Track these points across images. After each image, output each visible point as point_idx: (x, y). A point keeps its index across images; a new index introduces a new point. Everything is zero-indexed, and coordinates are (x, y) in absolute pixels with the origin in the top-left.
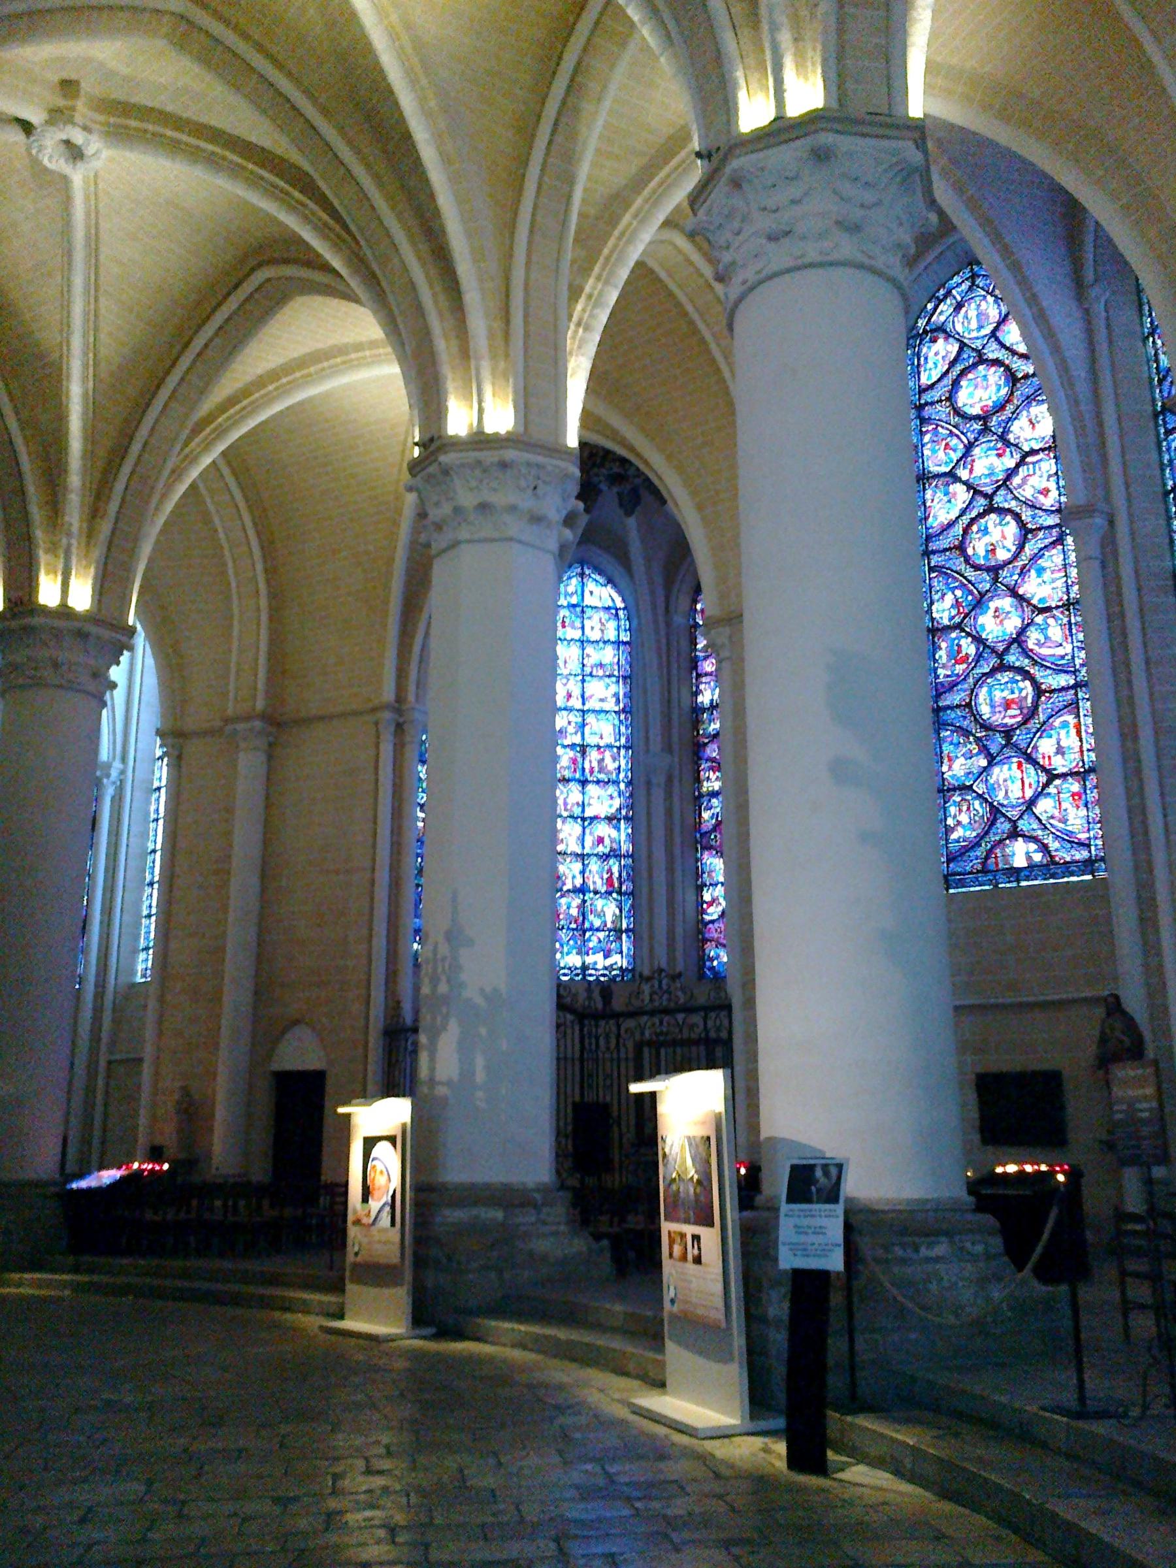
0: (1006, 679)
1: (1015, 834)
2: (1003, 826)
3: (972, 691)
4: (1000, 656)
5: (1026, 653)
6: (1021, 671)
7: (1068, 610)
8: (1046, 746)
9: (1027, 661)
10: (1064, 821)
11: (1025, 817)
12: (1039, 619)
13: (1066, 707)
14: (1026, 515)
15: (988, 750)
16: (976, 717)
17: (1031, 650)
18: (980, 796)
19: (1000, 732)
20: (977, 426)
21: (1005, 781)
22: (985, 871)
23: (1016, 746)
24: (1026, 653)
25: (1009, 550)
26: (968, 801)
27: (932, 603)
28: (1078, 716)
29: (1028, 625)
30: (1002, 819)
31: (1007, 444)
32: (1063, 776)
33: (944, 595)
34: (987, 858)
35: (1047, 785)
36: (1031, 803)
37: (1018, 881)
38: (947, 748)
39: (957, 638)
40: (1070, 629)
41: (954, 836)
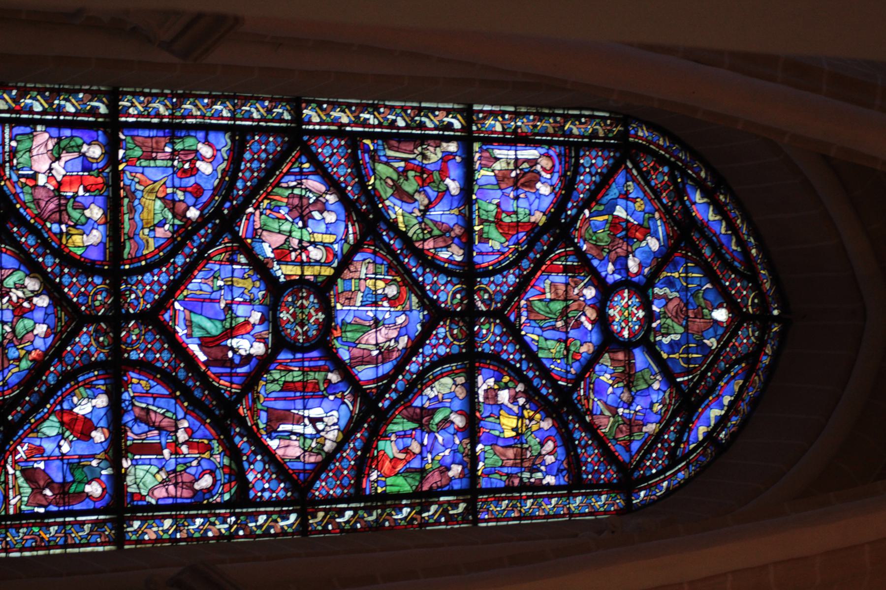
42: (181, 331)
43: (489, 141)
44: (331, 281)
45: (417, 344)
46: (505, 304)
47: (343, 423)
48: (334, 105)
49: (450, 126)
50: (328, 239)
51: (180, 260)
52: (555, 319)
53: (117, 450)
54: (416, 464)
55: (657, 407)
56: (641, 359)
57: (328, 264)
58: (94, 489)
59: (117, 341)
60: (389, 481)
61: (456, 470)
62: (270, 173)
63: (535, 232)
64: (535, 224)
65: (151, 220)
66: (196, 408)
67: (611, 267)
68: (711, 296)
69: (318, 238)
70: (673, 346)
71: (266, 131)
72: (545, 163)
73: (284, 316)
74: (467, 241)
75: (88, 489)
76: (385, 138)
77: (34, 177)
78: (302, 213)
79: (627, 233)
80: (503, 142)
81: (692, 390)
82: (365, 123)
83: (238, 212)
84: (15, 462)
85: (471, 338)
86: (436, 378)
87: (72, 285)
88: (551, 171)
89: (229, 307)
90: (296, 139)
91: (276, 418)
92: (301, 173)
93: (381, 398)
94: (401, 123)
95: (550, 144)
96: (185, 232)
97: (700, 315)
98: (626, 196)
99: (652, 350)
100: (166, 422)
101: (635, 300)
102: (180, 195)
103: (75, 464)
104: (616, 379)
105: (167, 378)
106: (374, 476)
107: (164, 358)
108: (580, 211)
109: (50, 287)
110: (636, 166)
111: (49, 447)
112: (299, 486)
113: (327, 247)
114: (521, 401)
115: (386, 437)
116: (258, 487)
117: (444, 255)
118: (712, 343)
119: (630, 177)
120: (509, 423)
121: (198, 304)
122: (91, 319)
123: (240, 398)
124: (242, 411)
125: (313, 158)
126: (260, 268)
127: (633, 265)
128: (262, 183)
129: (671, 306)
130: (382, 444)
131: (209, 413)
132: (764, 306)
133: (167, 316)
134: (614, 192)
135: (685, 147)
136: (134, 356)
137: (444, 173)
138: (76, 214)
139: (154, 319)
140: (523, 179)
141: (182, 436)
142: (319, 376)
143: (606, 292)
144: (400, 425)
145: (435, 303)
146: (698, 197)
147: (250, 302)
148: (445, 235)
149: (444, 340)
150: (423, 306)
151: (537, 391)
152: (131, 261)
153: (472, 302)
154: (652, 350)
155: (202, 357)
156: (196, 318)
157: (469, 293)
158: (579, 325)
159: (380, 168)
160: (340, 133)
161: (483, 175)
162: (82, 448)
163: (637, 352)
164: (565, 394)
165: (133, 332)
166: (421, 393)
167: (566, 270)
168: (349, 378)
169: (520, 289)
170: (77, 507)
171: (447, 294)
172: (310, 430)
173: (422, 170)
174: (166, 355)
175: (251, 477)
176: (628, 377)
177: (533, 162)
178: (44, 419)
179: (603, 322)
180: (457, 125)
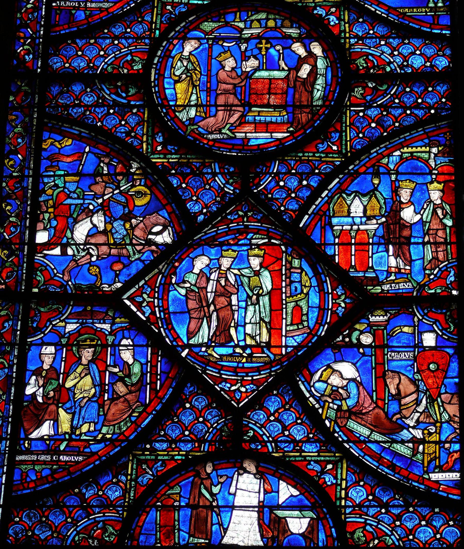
2: (199, 419)
3: (155, 44)
10: (391, 427)
11: (273, 404)
13: (420, 123)
15: (181, 204)
16: (160, 115)
18: (138, 327)
19: (223, 160)
21: (224, 292)
23: (263, 206)
30: (201, 402)
32: (400, 304)
34: (138, 507)
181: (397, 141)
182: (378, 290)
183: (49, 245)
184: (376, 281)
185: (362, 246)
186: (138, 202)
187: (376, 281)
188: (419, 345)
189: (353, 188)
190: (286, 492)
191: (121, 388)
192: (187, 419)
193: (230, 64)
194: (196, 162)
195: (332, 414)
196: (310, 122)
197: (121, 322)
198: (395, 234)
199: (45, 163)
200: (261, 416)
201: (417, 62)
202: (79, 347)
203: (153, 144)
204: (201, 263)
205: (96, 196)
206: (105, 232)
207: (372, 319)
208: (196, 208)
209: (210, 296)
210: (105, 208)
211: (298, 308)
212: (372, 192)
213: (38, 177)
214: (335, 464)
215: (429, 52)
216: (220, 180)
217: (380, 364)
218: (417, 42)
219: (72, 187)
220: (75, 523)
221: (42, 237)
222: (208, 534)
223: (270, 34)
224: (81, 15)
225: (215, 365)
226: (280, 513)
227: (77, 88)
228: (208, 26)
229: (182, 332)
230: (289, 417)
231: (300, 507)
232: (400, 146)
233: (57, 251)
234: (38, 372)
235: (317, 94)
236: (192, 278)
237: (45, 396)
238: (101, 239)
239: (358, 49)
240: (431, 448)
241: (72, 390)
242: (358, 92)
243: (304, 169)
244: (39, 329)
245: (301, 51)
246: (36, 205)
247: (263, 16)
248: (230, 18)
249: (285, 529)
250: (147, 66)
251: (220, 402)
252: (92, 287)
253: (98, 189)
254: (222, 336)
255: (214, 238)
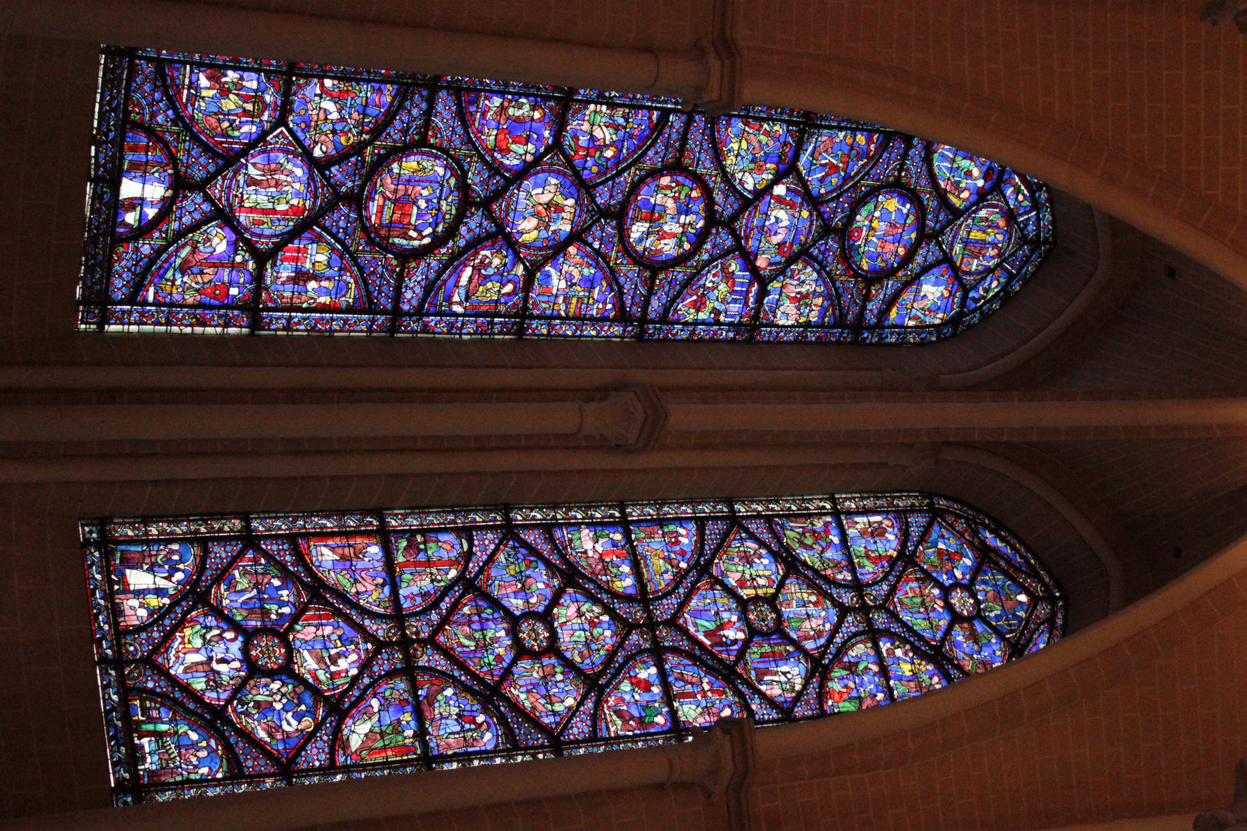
0: (444, 207)
1: (180, 185)
2: (200, 166)
4: (486, 204)
5: (475, 244)
6: (451, 232)
7: (515, 316)
8: (318, 256)
9: (462, 243)
10: (184, 269)
12: (520, 270)
13: (369, 293)
14: (679, 274)
17: (477, 253)
18: (262, 136)
20: (837, 221)
21: (278, 184)
22: (127, 124)
23: (331, 207)
24: (475, 244)
25: (640, 240)
26: (261, 114)
27: (612, 105)
28: (349, 310)
29: (516, 254)
30: (211, 168)
31: (792, 260)
32: (258, 277)
33: (617, 128)
34: (150, 132)
35: (251, 248)
36: (225, 217)
37: (96, 181)
38: (365, 92)
39: (540, 136)
40: (484, 315)
41: (204, 81)
42: (692, 629)
43: (849, 513)
44: (775, 596)
45: (836, 628)
46: (886, 600)
47: (803, 674)
48: (752, 502)
49: (824, 508)
50: (767, 573)
51: (681, 591)
52: (918, 607)
53: (669, 697)
54: (854, 694)
55: (998, 653)
56: (979, 627)
57: (770, 586)
58: (660, 720)
59: (654, 637)
60: (841, 705)
61: (880, 696)
62: (723, 540)
63: (892, 562)
64: (891, 557)
65: (660, 572)
66: (710, 670)
67: (945, 577)
68: (1013, 588)
69: (761, 573)
70: (997, 618)
71: (716, 519)
72: (887, 522)
73: (751, 617)
74: (852, 567)
75: (656, 720)
76: (788, 517)
77: (585, 552)
78: (748, 560)
79: (950, 558)
80: (858, 513)
81: (1018, 642)
82: (772, 510)
83: (710, 562)
84: (609, 707)
85: (869, 622)
86: (853, 645)
87: (621, 608)
88: (892, 526)
89: (717, 613)
90: (734, 522)
91: (761, 674)
92: (741, 538)
93: (824, 658)
94: (794, 508)
95: (887, 512)
96: (680, 577)
97: (1009, 598)
98: (943, 537)
99: (985, 621)
100: (694, 680)
101: (965, 594)
102: (673, 556)
103: (646, 706)
104: (967, 638)
105: (689, 655)
106: (830, 702)
107: (685, 645)
108: (917, 547)
109: (608, 610)
110: (944, 520)
111: (627, 697)
112: (785, 711)
113: (768, 578)
114: (911, 654)
115: (832, 680)
116: (760, 712)
117: (840, 577)
118: (1022, 614)
119: (941, 526)
120: (906, 668)
121: (697, 614)
122: (635, 626)
123: (736, 663)
124: (739, 670)
125: (747, 531)
126: (730, 592)
127: (958, 574)
128: (720, 546)
129: (990, 595)
130: (830, 684)
131: (721, 674)
132: (1048, 590)
133: (681, 621)
134: (934, 535)
135: (971, 507)
136: (666, 644)
137: (827, 532)
138: (614, 570)
139: (673, 622)
140: (878, 532)
141: (706, 687)
142: (782, 648)
143: (946, 592)
144: (838, 673)
145: (842, 604)
146: (988, 534)
147: (729, 610)
148: (837, 565)
149: (851, 624)
150: (835, 606)
151: (919, 649)
152: (653, 593)
153: (864, 601)
154: (985, 621)
155: (708, 643)
156: (699, 621)
157: (861, 597)
158: (934, 609)
159: (788, 532)
160: (759, 516)
161: (852, 532)
162: (647, 697)
163: (975, 622)
164: (938, 649)
165: (663, 632)
166: (846, 653)
167: (917, 580)
168: (800, 648)
169: (893, 590)
170: (652, 730)
171: (847, 598)
172: (783, 679)
173: (814, 532)
174: (686, 643)
175: (754, 707)
176: (974, 636)
177: (881, 523)
178: (620, 682)
179: (949, 607)
180: (828, 506)
181: (360, 281)
182: (268, 266)
183: (322, 85)
184: (274, 265)
185: (297, 259)
186: (343, 139)
187: (274, 265)
188: (231, 284)
189: (334, 256)
190: (151, 212)
191: (226, 124)
192: (202, 160)
193: (425, 193)
194: (364, 171)
195: (196, 238)
196: (380, 236)
197: (267, 126)
198: (301, 277)
199: (377, 86)
200: (199, 200)
201: (408, 295)
202: (254, 103)
203: (380, 148)
204: (299, 172)
205: (350, 114)
206: (326, 119)
207: (251, 263)
208: (333, 169)
209: (277, 177)
210: (342, 119)
211: (263, 223)
212: (329, 266)
213: (368, 81)
214: (166, 238)
215: (414, 302)
216: (350, 184)
217: (223, 265)
218: (421, 295)
219: (358, 101)
220: (145, 98)
221: (328, 83)
222: (128, 171)
223: (440, 216)
224: (472, 109)
225: (234, 176)
226: (138, 209)
227: (424, 106)
228: (453, 181)
229: (257, 160)
230: (197, 216)
231: (140, 220)
232: (356, 283)
233: (318, 91)
234: (242, 78)
235: (397, 240)
236: (290, 166)
237: (226, 83)
238: (322, 116)
239: (423, 263)
240: (168, 288)
241: (228, 97)
242: (394, 262)
243: (350, 231)
244: (268, 79)
245: (425, 233)
246: (349, 80)
247: (454, 212)
248: (456, 193)
249: (127, 211)
250: (432, 146)
251: (211, 178)
252: (292, 111)
253: (355, 115)
254: (251, 182)
255: (313, 179)
